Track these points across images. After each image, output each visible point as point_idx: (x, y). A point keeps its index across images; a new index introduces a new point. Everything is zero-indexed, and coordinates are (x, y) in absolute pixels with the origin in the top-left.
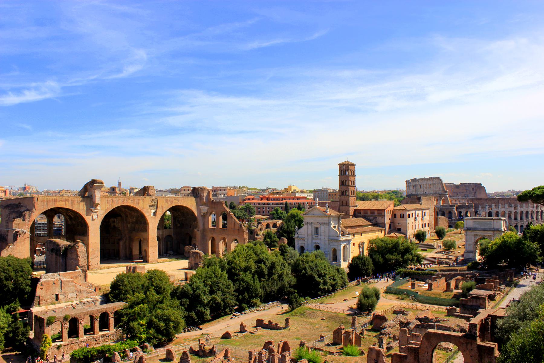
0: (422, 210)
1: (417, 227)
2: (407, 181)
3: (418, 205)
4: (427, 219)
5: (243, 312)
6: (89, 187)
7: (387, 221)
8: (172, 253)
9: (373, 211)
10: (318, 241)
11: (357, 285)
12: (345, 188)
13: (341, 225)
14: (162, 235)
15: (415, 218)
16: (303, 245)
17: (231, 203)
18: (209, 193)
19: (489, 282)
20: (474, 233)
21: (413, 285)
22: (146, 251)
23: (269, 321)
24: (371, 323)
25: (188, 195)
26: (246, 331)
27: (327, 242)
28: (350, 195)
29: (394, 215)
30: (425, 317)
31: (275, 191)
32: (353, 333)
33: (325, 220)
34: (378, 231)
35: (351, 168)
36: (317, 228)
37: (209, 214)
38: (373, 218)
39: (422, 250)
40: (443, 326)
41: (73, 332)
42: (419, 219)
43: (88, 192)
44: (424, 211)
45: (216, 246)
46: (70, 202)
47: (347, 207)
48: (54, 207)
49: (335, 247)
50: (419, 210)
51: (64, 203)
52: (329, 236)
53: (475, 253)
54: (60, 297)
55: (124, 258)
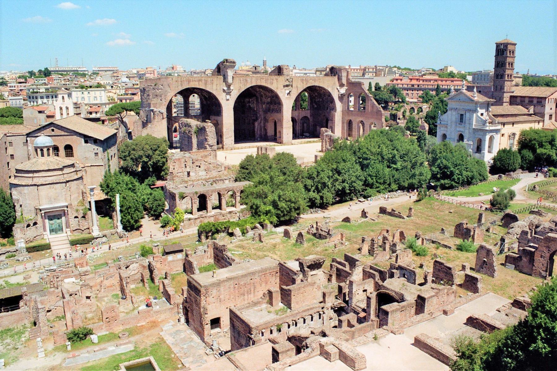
5: (369, 199)
6: (221, 66)
8: (307, 134)
10: (462, 129)
14: (298, 116)
16: (445, 132)
22: (280, 132)
23: (393, 210)
25: (326, 75)
28: (506, 78)
33: (471, 106)
34: (535, 121)
35: (510, 47)
36: (462, 115)
41: (203, 206)
43: (220, 70)
46: (203, 81)
48: (188, 87)
49: (480, 137)
51: (197, 83)
54: (191, 174)
55: (259, 139)
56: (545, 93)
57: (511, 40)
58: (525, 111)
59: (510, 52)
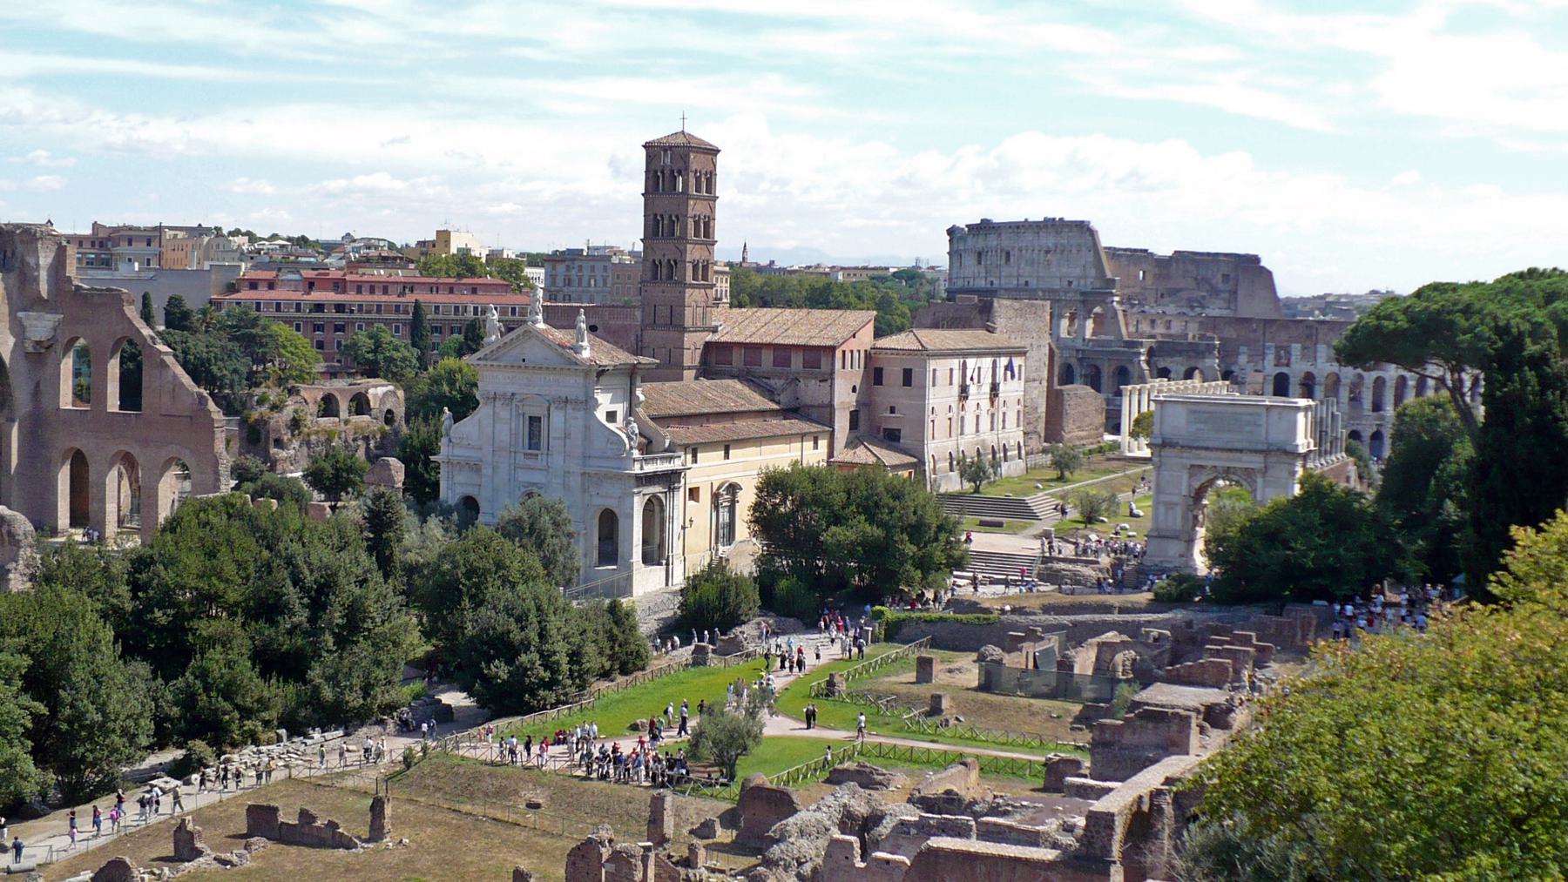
0: (995, 353)
1: (970, 427)
2: (951, 232)
3: (982, 333)
4: (1012, 390)
7: (844, 394)
9: (782, 352)
10: (538, 477)
11: (696, 663)
12: (666, 251)
13: (640, 410)
15: (964, 390)
17: (174, 302)
18: (61, 253)
19: (1218, 653)
20: (1190, 459)
21: (924, 667)
24: (729, 819)
26: (199, 853)
27: (575, 482)
28: (689, 279)
29: (874, 374)
30: (948, 792)
31: (373, 253)
32: (645, 859)
33: (571, 386)
34: (802, 437)
35: (696, 162)
36: (535, 421)
37: (59, 348)
38: (786, 384)
39: (983, 524)
40: (1011, 828)
42: (979, 394)
44: (1004, 361)
45: (93, 491)
47: (673, 334)
49: (611, 504)
50: (980, 354)
52: (586, 457)
53: (1190, 541)
56: (831, 331)
57: (705, 133)
58: (760, 402)
59: (698, 180)
